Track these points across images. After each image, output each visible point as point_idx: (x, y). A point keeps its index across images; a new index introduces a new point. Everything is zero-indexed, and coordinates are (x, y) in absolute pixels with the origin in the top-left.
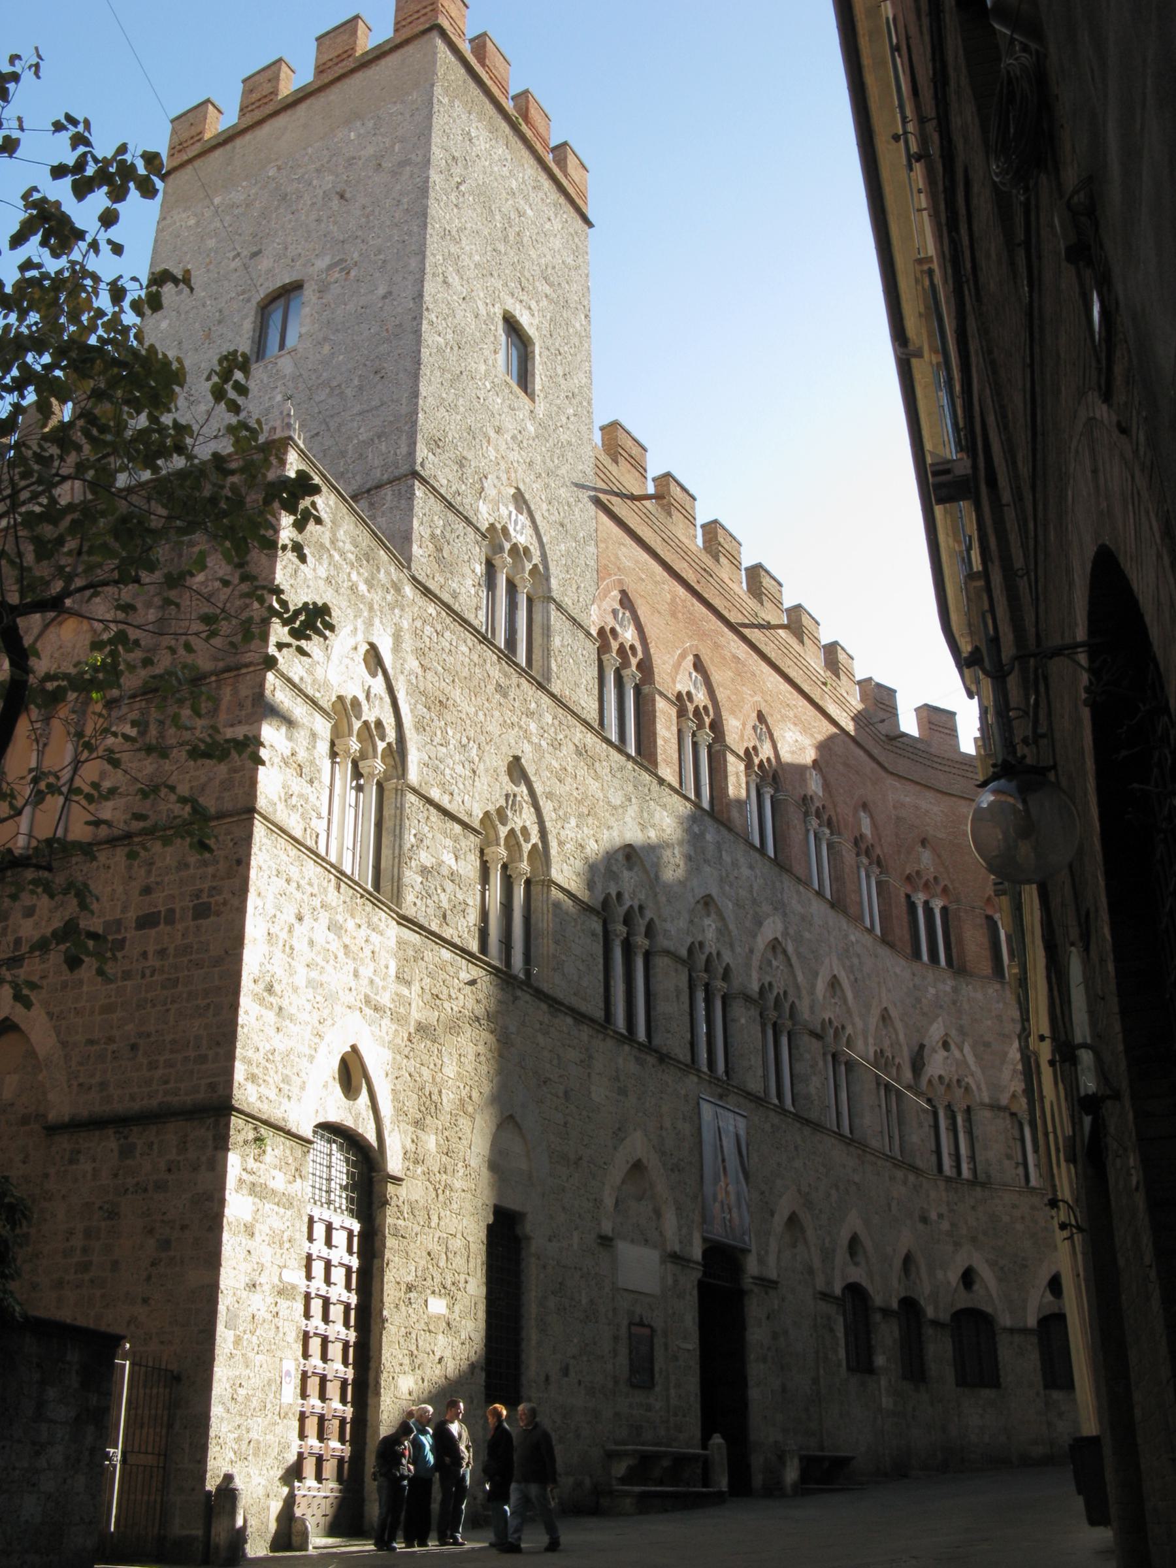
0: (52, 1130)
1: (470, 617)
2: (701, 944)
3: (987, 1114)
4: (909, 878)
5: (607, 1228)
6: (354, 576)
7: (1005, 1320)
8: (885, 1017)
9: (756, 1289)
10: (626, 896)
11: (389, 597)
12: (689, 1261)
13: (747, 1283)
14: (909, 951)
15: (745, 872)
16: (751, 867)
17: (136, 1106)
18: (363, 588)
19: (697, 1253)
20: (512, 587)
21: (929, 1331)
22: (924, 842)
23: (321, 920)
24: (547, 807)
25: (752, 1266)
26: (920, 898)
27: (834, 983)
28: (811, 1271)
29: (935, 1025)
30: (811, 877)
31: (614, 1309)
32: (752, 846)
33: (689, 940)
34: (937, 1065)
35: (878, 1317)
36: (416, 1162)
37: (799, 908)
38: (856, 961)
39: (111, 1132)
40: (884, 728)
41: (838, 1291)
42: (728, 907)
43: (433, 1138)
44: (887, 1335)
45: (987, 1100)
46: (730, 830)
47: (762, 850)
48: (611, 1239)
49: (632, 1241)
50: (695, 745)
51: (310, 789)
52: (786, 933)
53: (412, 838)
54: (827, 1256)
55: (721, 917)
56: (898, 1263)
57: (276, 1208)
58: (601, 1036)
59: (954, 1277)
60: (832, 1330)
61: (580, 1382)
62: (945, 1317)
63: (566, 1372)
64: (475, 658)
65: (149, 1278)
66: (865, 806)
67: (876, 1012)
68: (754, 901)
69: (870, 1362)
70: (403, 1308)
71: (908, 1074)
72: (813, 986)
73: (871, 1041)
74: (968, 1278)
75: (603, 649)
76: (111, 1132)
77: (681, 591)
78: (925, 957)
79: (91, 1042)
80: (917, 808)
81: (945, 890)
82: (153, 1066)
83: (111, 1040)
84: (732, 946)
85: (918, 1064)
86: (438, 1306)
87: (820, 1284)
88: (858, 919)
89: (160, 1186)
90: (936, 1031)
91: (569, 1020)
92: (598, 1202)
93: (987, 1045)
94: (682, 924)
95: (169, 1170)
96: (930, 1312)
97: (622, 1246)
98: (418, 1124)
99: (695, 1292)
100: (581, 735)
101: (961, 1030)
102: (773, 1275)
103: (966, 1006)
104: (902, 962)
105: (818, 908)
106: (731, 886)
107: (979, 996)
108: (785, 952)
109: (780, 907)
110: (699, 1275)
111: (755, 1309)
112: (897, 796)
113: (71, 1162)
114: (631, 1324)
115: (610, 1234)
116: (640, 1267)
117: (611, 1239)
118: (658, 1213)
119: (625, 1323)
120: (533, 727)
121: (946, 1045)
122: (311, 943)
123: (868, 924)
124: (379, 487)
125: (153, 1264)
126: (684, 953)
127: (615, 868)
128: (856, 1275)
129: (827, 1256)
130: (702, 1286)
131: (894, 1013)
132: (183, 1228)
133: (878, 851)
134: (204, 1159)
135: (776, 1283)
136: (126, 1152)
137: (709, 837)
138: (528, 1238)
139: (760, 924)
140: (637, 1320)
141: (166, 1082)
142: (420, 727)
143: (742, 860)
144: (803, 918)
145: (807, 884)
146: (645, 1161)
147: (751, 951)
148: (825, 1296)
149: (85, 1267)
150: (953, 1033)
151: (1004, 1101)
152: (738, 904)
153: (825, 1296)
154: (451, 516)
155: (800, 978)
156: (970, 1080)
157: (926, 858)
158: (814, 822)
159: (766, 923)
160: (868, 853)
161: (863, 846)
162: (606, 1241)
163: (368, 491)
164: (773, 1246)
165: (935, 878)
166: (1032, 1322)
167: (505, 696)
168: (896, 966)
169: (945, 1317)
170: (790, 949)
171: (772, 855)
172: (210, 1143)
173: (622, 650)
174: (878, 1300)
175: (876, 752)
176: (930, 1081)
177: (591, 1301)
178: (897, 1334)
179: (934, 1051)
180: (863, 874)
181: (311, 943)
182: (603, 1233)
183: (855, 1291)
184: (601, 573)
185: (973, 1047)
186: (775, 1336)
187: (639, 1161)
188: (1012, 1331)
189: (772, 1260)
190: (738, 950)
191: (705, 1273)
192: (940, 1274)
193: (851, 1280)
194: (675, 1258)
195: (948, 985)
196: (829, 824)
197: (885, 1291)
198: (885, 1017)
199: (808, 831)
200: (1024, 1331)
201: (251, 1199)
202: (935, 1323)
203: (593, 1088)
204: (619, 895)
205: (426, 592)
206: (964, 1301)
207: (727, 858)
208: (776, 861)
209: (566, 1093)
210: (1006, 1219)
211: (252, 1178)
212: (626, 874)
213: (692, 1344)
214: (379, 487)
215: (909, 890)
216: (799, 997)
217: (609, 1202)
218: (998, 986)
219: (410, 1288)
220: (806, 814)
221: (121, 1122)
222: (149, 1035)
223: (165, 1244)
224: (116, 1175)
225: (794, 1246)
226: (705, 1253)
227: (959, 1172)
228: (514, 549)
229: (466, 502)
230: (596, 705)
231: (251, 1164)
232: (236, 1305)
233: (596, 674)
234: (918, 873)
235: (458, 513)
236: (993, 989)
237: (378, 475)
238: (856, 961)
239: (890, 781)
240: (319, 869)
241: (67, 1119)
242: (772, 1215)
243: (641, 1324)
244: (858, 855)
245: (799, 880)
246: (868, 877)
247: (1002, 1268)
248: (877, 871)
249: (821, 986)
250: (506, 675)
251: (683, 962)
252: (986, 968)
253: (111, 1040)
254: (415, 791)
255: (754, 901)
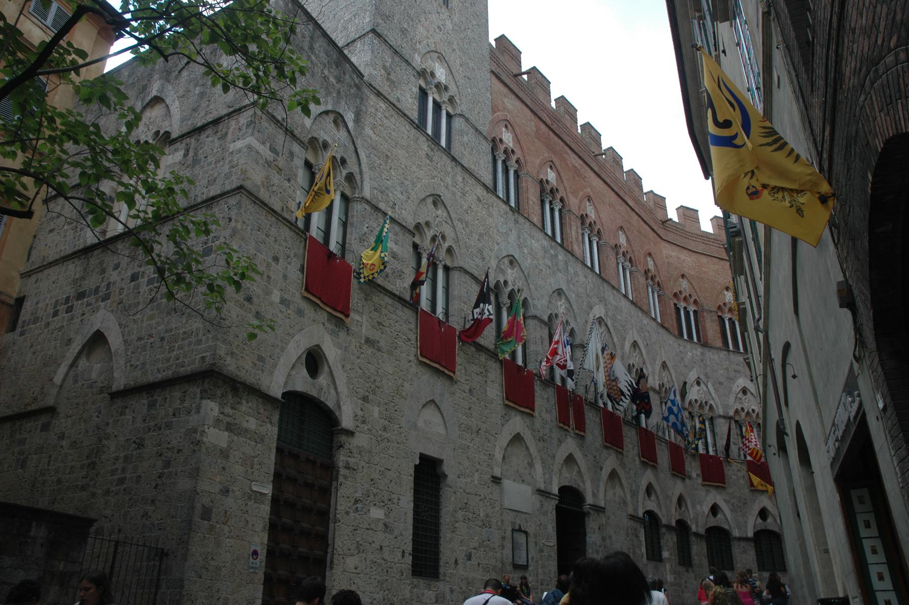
0: (114, 396)
1: (410, 115)
2: (556, 315)
3: (722, 420)
4: (675, 295)
5: (497, 472)
6: (326, 72)
7: (736, 533)
8: (664, 366)
9: (592, 512)
10: (510, 283)
11: (352, 91)
12: (550, 494)
13: (586, 508)
14: (676, 333)
15: (582, 279)
16: (585, 277)
17: (159, 377)
18: (332, 80)
19: (555, 490)
20: (437, 106)
21: (693, 539)
22: (683, 276)
23: (293, 264)
24: (459, 226)
25: (589, 499)
26: (682, 305)
27: (635, 345)
28: (625, 503)
29: (692, 373)
30: (620, 285)
31: (502, 521)
32: (586, 266)
33: (550, 312)
34: (694, 394)
35: (663, 530)
36: (364, 422)
37: (614, 302)
38: (647, 334)
39: (144, 394)
40: (660, 216)
41: (641, 515)
42: (572, 297)
43: (376, 410)
44: (669, 541)
45: (722, 413)
46: (573, 255)
47: (592, 269)
48: (500, 479)
49: (514, 480)
50: (552, 210)
51: (288, 184)
52: (606, 315)
53: (365, 228)
54: (634, 494)
55: (567, 299)
56: (675, 500)
57: (249, 441)
58: (493, 360)
59: (706, 508)
60: (637, 536)
61: (479, 564)
62: (702, 531)
63: (469, 557)
64: (412, 136)
65: (157, 485)
66: (650, 254)
67: (659, 364)
68: (588, 295)
69: (661, 556)
70: (352, 514)
71: (678, 398)
72: (623, 346)
73: (657, 378)
74: (715, 509)
75: (494, 149)
76: (144, 394)
77: (543, 127)
78: (686, 337)
79: (140, 339)
80: (679, 258)
81: (695, 302)
82: (171, 350)
83: (151, 336)
84: (575, 317)
85: (683, 394)
86: (377, 513)
87: (630, 511)
88: (647, 313)
89: (169, 426)
90: (692, 376)
91: (473, 349)
92: (491, 456)
93: (721, 383)
94: (544, 302)
95: (174, 415)
96: (694, 528)
97: (506, 483)
98: (365, 399)
99: (554, 512)
100: (480, 191)
101: (706, 375)
102: (602, 504)
103: (708, 363)
104: (673, 338)
105: (624, 303)
106: (574, 285)
107: (716, 357)
108: (606, 325)
109: (603, 300)
110: (557, 502)
111: (592, 524)
112: (668, 252)
113: (121, 414)
114: (513, 530)
115: (499, 476)
116: (518, 495)
117: (500, 479)
118: (531, 465)
119: (510, 529)
120: (449, 180)
121: (698, 383)
122: (285, 277)
123: (653, 316)
124: (354, 41)
125: (160, 477)
126: (546, 318)
127: (502, 267)
128: (651, 505)
129: (634, 494)
130: (558, 508)
131: (669, 365)
132: (179, 451)
133: (657, 279)
134: (194, 405)
135: (604, 508)
136: (152, 405)
137: (560, 257)
138: (446, 476)
139: (592, 308)
140: (517, 527)
141: (178, 359)
142: (372, 168)
143: (580, 273)
144: (616, 308)
145: (618, 291)
146: (522, 434)
147: (586, 322)
148: (633, 517)
149: (121, 481)
150: (702, 377)
151: (731, 413)
152: (577, 295)
153: (633, 517)
154: (397, 59)
155: (615, 340)
156: (712, 402)
157: (684, 284)
158: (622, 259)
159: (595, 308)
160: (652, 279)
161: (650, 275)
162: (496, 480)
163: (348, 45)
164: (602, 488)
165: (690, 295)
166: (750, 534)
167: (431, 161)
168: (670, 340)
169: (702, 531)
170: (609, 324)
171: (598, 272)
172: (198, 395)
173: (505, 151)
174: (664, 521)
175: (655, 228)
176: (690, 403)
177: (487, 516)
178: (675, 539)
179: (692, 386)
180: (650, 290)
181: (285, 277)
182: (495, 475)
183: (650, 513)
184: (494, 110)
185: (713, 385)
186: (604, 539)
187: (518, 434)
188: (740, 539)
189: (601, 495)
190: (579, 320)
191: (560, 502)
192: (698, 507)
193: (648, 509)
194: (540, 492)
195: (700, 350)
196: (630, 260)
197: (668, 515)
198: (664, 366)
199: (618, 263)
200: (747, 539)
201: (226, 433)
202: (697, 535)
203: (488, 389)
204: (506, 282)
205: (379, 94)
206: (712, 522)
207: (571, 270)
208: (600, 276)
209: (470, 390)
210: (734, 477)
211: (228, 419)
212: (509, 271)
213: (553, 542)
214: (354, 41)
215: (676, 301)
216: (616, 351)
217: (499, 456)
218: (726, 353)
219: (356, 501)
220: (617, 254)
221: (149, 388)
222: (171, 330)
223: (167, 464)
224: (144, 420)
225: (614, 488)
226: (559, 490)
227: (708, 451)
228: (438, 86)
229: (406, 52)
230: (491, 177)
231: (228, 410)
232: (211, 504)
233: (491, 161)
234: (680, 292)
235: (401, 57)
236: (723, 354)
237: (353, 36)
238: (647, 334)
239: (663, 244)
240: (293, 233)
241: (122, 388)
242: (601, 469)
243: (520, 530)
244: (647, 279)
245: (614, 287)
246: (653, 292)
247: (733, 504)
248: (658, 289)
249: (627, 345)
250: (432, 150)
251: (545, 324)
252: (719, 343)
253: (151, 336)
254: (368, 202)
255: (588, 295)
